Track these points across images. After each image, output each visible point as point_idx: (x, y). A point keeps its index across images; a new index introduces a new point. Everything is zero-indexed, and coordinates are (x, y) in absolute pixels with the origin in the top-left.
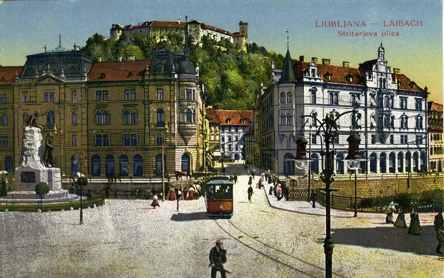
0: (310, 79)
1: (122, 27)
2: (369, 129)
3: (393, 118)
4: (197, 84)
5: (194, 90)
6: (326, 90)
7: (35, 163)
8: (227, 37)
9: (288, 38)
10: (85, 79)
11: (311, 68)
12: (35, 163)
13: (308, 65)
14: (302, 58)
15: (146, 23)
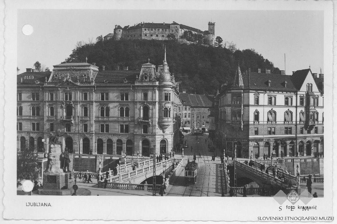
1: (123, 27)
2: (298, 123)
3: (317, 114)
5: (170, 93)
6: (266, 95)
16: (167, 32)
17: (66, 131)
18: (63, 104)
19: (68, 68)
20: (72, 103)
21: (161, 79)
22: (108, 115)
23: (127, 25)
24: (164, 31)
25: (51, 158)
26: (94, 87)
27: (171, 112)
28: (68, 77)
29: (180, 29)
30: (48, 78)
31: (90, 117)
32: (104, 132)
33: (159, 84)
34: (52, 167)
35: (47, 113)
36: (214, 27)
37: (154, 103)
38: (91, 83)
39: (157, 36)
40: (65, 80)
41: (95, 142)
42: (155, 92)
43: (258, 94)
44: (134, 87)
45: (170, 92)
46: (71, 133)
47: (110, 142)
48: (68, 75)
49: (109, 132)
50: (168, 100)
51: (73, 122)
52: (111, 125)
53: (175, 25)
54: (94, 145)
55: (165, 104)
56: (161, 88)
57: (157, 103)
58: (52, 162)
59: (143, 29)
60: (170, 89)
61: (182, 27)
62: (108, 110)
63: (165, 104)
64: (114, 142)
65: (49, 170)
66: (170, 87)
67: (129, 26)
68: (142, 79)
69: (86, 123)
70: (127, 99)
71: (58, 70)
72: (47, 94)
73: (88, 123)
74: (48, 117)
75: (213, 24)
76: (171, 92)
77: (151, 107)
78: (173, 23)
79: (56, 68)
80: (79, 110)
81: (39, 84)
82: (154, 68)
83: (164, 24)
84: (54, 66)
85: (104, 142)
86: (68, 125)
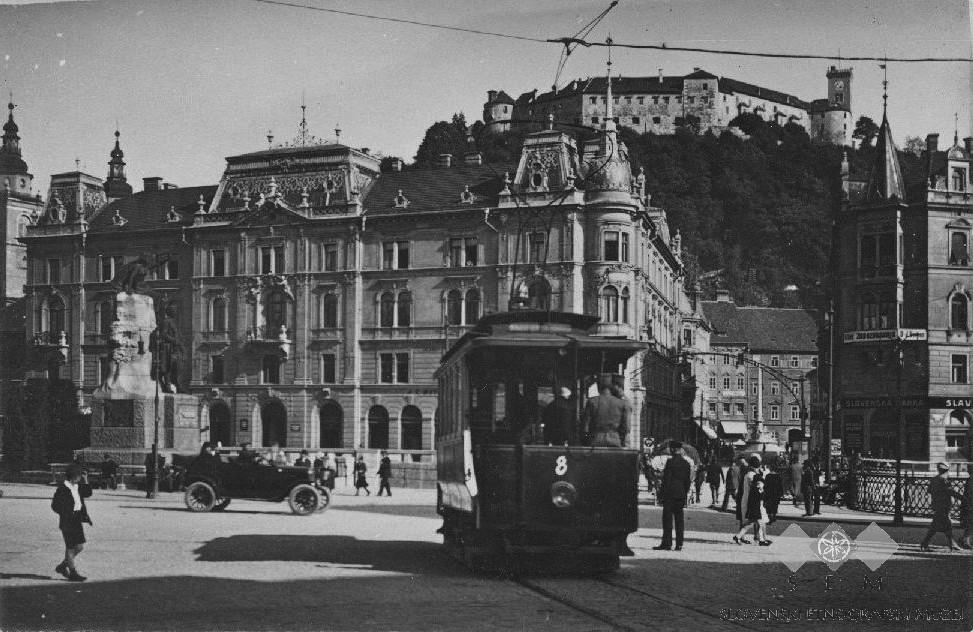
0: (948, 196)
1: (515, 97)
4: (634, 219)
5: (625, 235)
7: (134, 379)
8: (796, 112)
9: (885, 83)
10: (355, 211)
11: (951, 164)
12: (134, 379)
13: (944, 157)
14: (932, 139)
15: (573, 83)
16: (675, 107)
17: (265, 381)
18: (256, 287)
19: (276, 162)
20: (285, 282)
21: (593, 181)
22: (404, 319)
23: (531, 90)
24: (661, 101)
25: (119, 338)
26: (358, 220)
27: (631, 303)
28: (274, 190)
29: (722, 95)
30: (209, 202)
31: (344, 331)
32: (391, 380)
33: (586, 198)
34: (122, 372)
35: (203, 321)
36: (847, 86)
37: (564, 268)
38: (352, 210)
39: (636, 120)
40: (261, 202)
41: (363, 419)
42: (571, 230)
43: (963, 225)
44: (496, 216)
45: (624, 229)
46: (283, 390)
47: (412, 415)
48: (272, 184)
49: (411, 382)
50: (616, 259)
51: (286, 348)
52: (415, 356)
53: (704, 81)
54: (358, 429)
55: (608, 272)
56: (591, 215)
57: (577, 272)
58: (122, 352)
59: (586, 98)
60: (627, 217)
61: (728, 86)
62: (406, 301)
63: (608, 272)
64: (424, 416)
65: (110, 381)
66: (626, 212)
67: (536, 91)
68: (525, 183)
69: (330, 352)
70: (472, 255)
71: (242, 172)
72: (204, 253)
73: (337, 351)
74: (206, 335)
75: (846, 75)
76: (630, 230)
77: (555, 283)
78: (693, 71)
79: (234, 168)
80: (309, 311)
81: (179, 223)
82: (570, 149)
83: (661, 81)
84: (231, 161)
85: (390, 416)
86: (268, 357)
